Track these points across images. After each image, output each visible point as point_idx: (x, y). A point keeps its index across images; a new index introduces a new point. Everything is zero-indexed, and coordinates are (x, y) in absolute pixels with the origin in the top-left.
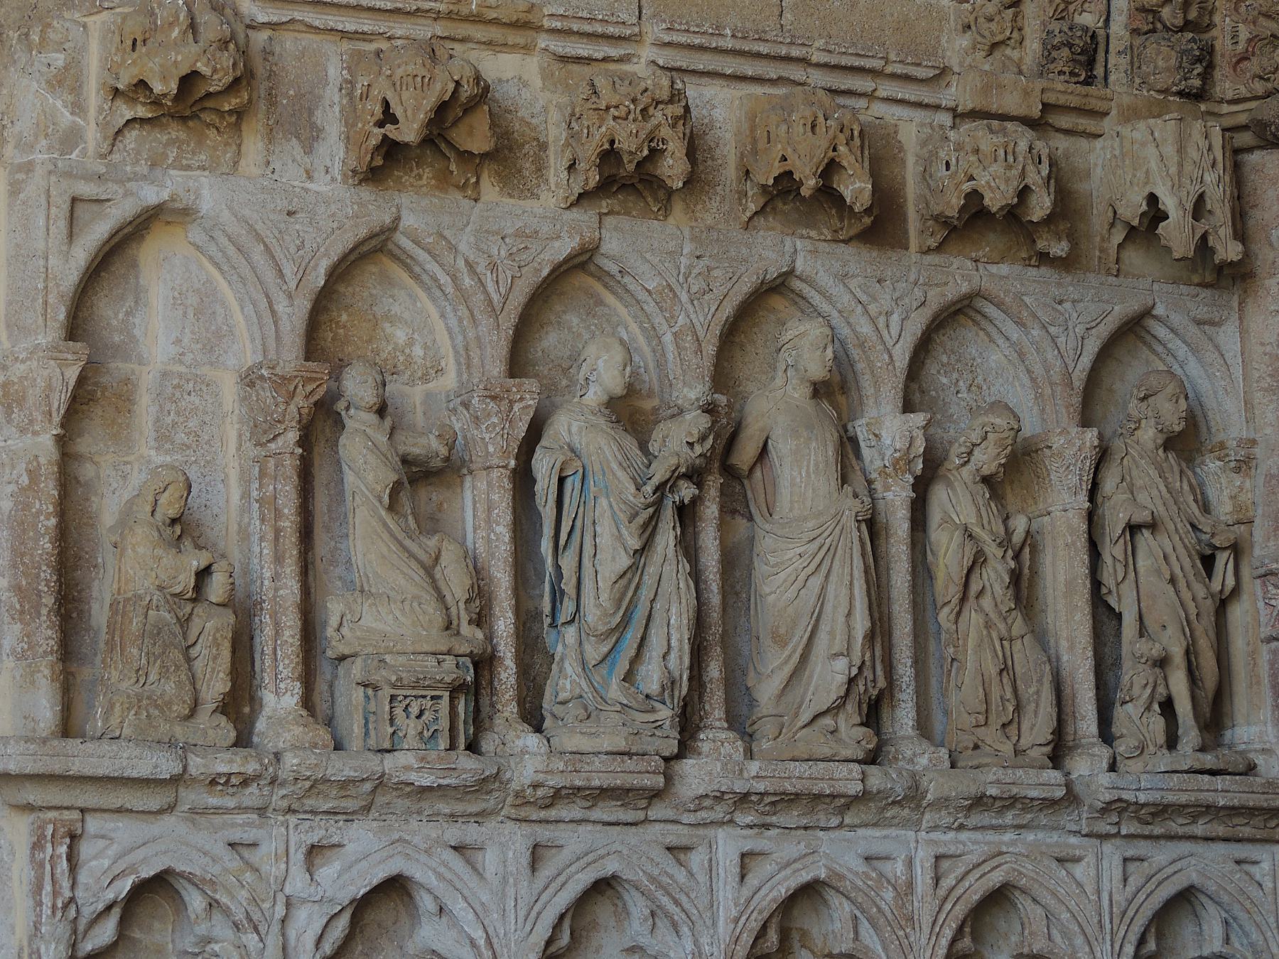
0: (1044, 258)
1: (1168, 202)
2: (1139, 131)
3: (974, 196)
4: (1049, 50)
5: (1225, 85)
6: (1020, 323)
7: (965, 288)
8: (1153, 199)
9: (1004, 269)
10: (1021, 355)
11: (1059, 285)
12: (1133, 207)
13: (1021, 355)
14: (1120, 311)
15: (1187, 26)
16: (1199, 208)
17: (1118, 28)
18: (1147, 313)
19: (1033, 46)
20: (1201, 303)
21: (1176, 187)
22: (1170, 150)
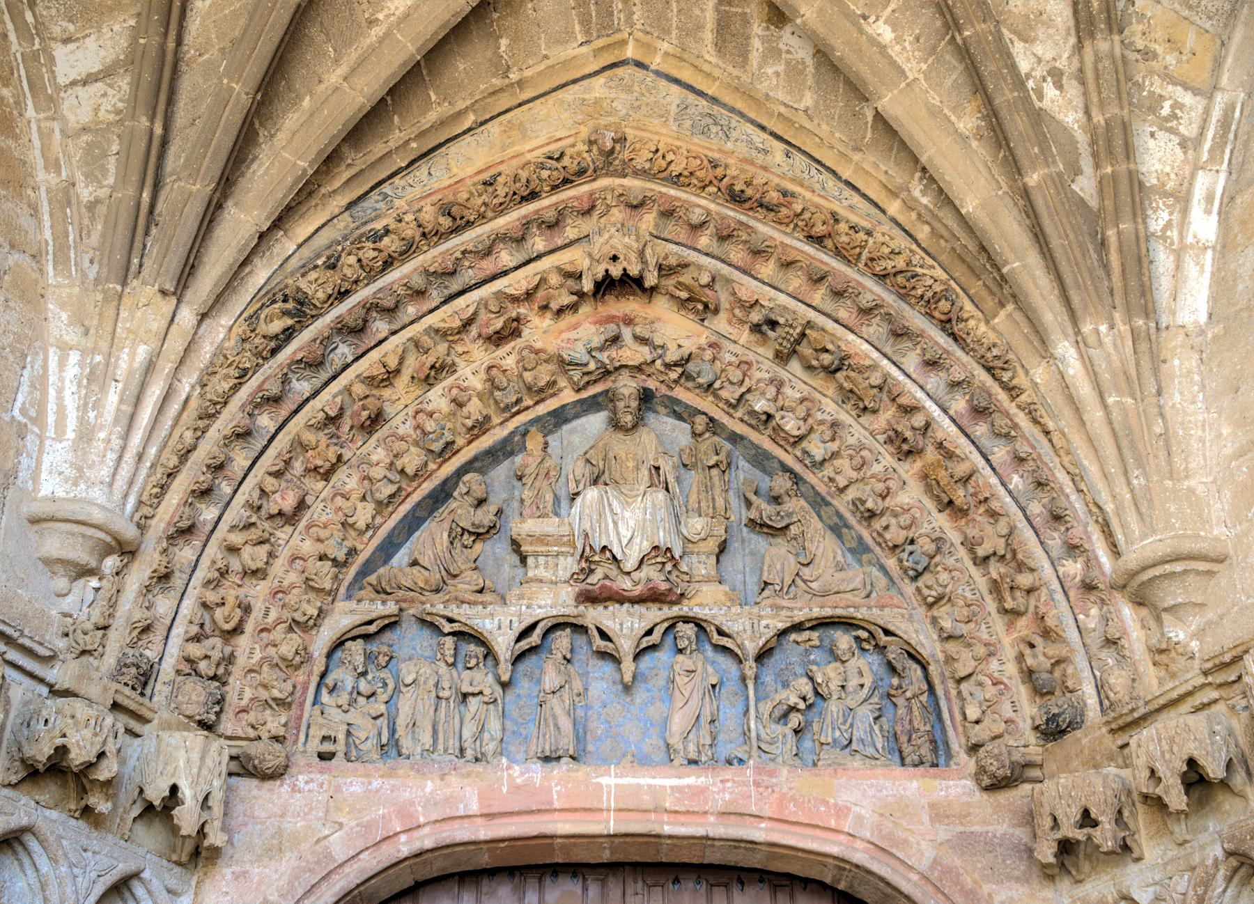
0: (87, 812)
1: (186, 792)
2: (174, 739)
3: (62, 750)
4: (122, 665)
5: (228, 725)
6: (53, 860)
7: (25, 821)
8: (174, 789)
9: (54, 814)
10: (43, 888)
11: (88, 837)
12: (157, 793)
13: (43, 888)
14: (122, 868)
15: (214, 678)
16: (205, 803)
17: (168, 667)
18: (136, 875)
19: (110, 661)
20: (174, 876)
21: (194, 784)
22: (195, 756)
